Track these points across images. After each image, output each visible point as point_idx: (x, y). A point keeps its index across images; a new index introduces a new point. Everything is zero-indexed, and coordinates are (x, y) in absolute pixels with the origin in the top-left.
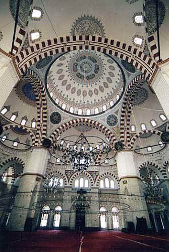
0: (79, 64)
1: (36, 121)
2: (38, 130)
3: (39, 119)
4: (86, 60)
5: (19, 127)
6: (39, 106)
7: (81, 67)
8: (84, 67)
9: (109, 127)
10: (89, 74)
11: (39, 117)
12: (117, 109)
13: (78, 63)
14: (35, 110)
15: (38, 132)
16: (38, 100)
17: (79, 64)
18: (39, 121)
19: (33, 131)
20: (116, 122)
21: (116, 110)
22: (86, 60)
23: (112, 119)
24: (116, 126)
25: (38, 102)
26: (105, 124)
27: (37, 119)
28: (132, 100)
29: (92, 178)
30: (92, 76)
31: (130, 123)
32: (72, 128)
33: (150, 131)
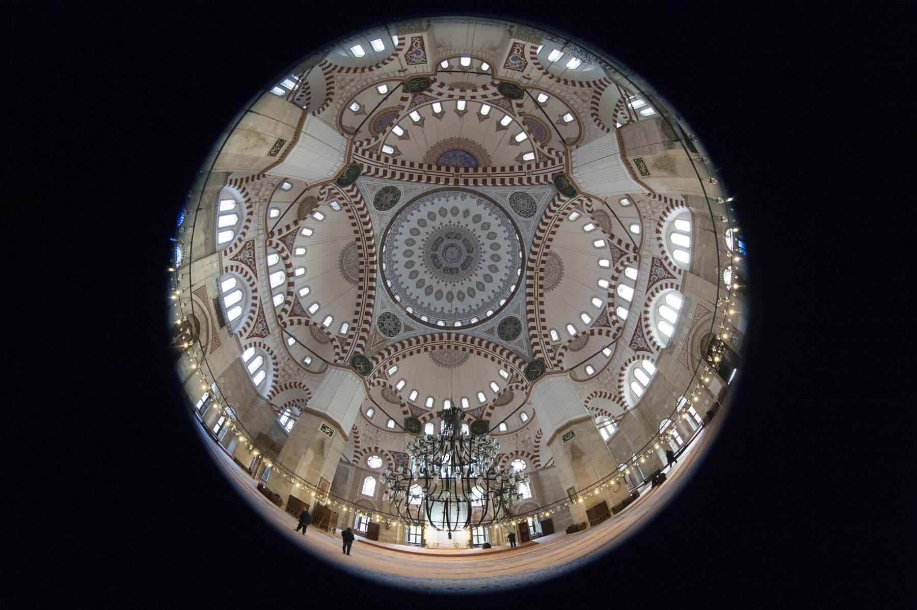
0: (459, 243)
1: (393, 155)
2: (378, 158)
3: (399, 163)
4: (465, 254)
5: (395, 121)
6: (425, 167)
7: (452, 245)
8: (452, 249)
9: (375, 322)
10: (440, 258)
11: (403, 163)
12: (414, 327)
14: (418, 159)
15: (375, 156)
16: (439, 168)
18: (395, 162)
19: (377, 145)
20: (390, 333)
21: (412, 326)
22: (465, 254)
25: (434, 168)
26: (378, 312)
28: (441, 347)
29: (252, 324)
31: (402, 361)
32: (352, 238)
33: (400, 398)
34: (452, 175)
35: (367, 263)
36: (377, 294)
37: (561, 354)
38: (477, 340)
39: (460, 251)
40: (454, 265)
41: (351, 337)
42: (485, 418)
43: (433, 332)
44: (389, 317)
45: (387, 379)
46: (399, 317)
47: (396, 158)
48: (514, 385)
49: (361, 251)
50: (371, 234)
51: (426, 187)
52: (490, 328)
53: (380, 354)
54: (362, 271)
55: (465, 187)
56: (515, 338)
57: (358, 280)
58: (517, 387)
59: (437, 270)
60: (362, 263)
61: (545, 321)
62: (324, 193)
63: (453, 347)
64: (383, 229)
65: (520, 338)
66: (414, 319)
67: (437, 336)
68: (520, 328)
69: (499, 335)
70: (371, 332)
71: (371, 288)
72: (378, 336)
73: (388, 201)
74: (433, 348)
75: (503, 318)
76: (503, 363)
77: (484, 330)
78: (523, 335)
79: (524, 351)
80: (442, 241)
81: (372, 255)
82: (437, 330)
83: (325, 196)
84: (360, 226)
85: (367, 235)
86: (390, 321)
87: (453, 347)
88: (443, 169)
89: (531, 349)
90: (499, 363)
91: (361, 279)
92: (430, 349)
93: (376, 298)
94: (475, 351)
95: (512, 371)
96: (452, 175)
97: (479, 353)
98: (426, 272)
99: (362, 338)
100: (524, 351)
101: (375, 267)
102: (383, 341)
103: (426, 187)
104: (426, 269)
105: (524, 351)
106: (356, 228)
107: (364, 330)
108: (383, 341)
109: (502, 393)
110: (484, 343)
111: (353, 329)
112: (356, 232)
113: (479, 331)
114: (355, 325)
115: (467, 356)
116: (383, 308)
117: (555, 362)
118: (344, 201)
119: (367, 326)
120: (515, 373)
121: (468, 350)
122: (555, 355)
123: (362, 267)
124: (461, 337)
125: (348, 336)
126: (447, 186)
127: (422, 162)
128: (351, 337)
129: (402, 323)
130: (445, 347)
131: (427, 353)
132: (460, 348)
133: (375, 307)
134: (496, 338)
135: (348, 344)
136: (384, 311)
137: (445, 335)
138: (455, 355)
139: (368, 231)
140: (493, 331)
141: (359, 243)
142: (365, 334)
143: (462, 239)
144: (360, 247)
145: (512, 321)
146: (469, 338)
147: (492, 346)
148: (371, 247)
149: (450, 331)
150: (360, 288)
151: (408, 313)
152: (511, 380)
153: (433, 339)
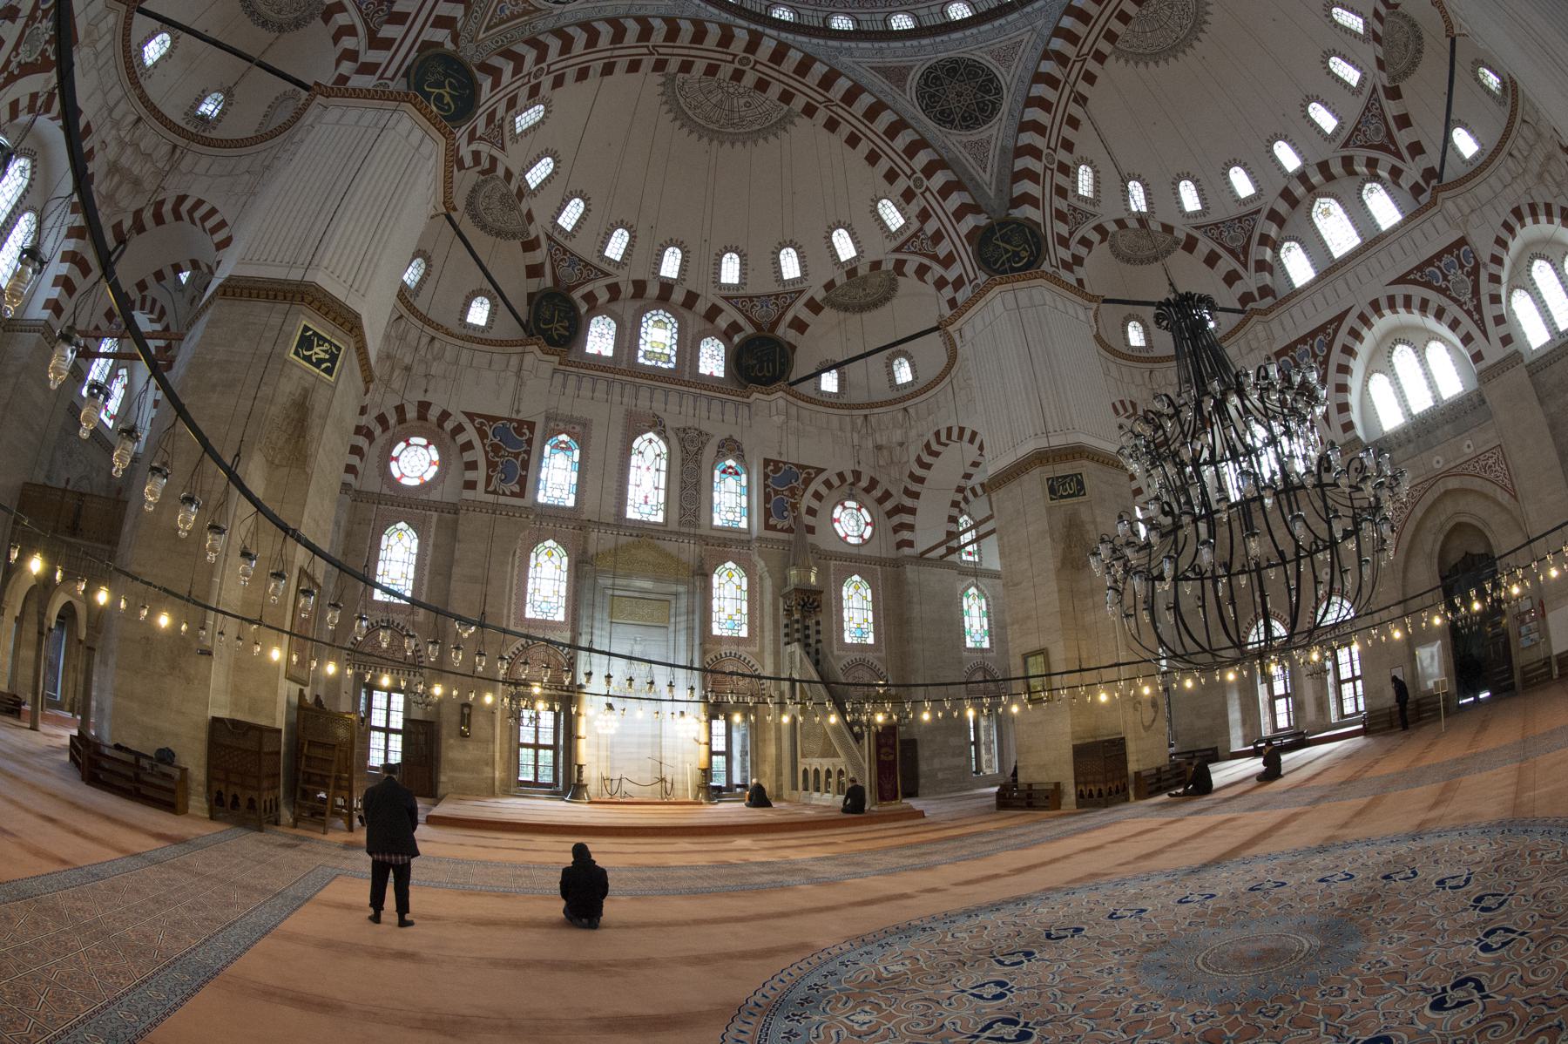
28: (712, 70)
37: (1085, 242)
38: (843, 85)
42: (784, 332)
45: (503, 148)
48: (913, 262)
52: (891, 61)
56: (968, 128)
58: (922, 271)
61: (1076, 129)
63: (750, 79)
65: (985, 136)
67: (714, 32)
68: (995, 109)
69: (920, 96)
74: (686, 67)
75: (952, 54)
76: (902, 183)
77: (877, 61)
78: (996, 132)
79: (987, 177)
87: (750, 79)
89: (1008, 181)
90: (891, 176)
92: (673, 65)
94: (822, 115)
95: (924, 216)
97: (832, 125)
100: (987, 177)
105: (987, 178)
109: (863, 270)
110: (865, 100)
113: (859, 61)
117: (1066, 255)
120: (931, 227)
121: (799, 102)
122: (1071, 234)
124: (794, 57)
130: (726, 71)
131: (657, 78)
132: (775, 90)
134: (907, 102)
137: (742, 37)
140: (905, 78)
145: (976, 75)
146: (819, 69)
147: (886, 118)
149: (760, 29)
152: (906, 242)
153: (699, 35)
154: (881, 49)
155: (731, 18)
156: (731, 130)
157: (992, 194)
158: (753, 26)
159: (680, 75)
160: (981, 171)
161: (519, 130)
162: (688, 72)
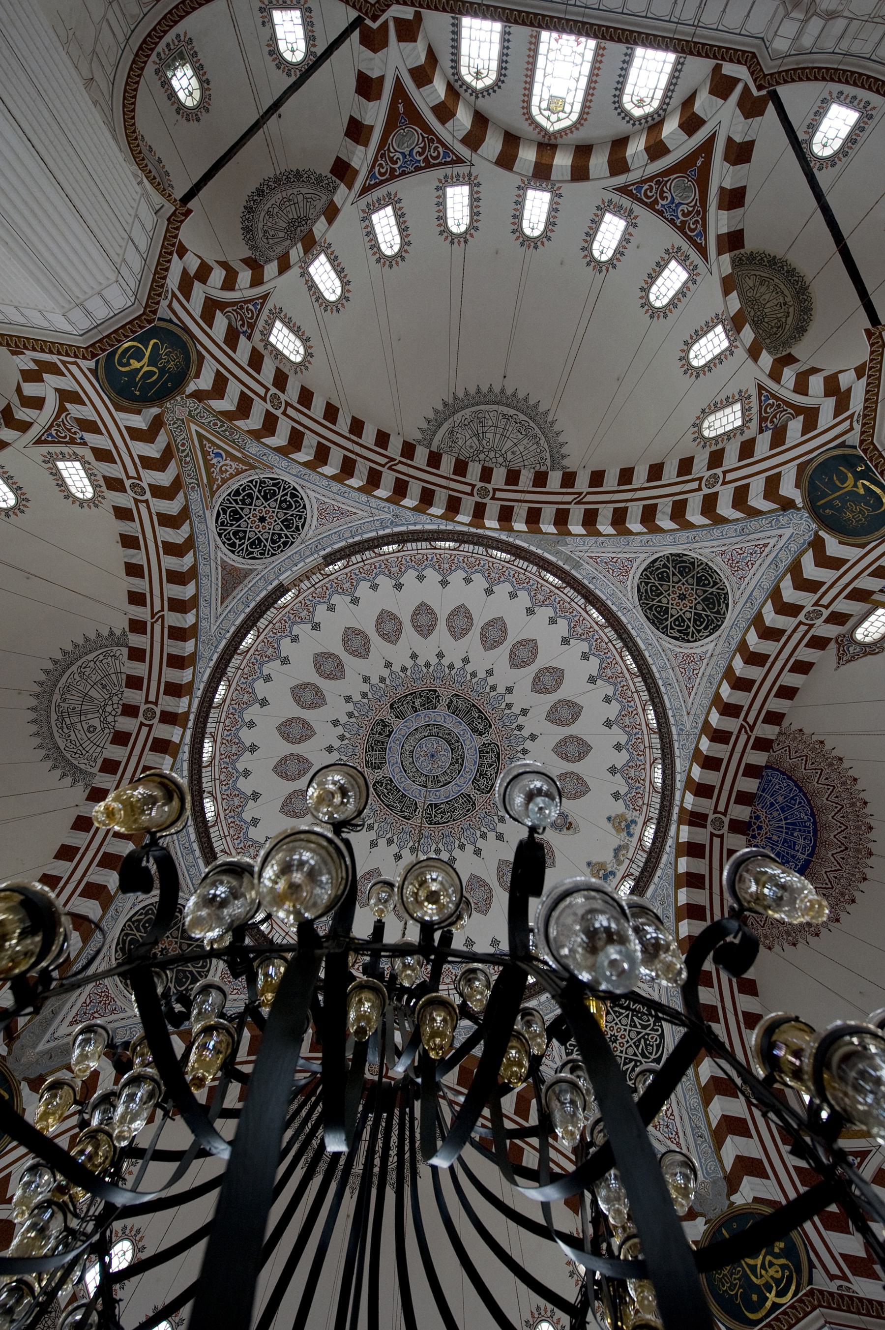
6: (769, 731)
8: (445, 757)
10: (424, 718)
11: (802, 668)
12: (231, 602)
13: (468, 788)
16: (752, 771)
17: (464, 784)
18: (819, 643)
21: (240, 593)
23: (264, 532)
24: (223, 494)
25: (759, 758)
27: (824, 658)
28: (134, 682)
30: (406, 708)
34: (721, 808)
35: (484, 492)
36: (374, 502)
39: (436, 780)
40: (394, 755)
41: (256, 361)
43: (200, 665)
44: (287, 524)
46: (282, 557)
47: (833, 645)
49: (526, 479)
50: (577, 529)
51: (688, 722)
53: (168, 454)
54: (461, 468)
55: (670, 842)
57: (434, 448)
59: (386, 701)
60: (486, 475)
62: (801, 387)
63: (127, 724)
64: (577, 565)
66: (259, 605)
70: (253, 448)
71: (401, 489)
72: (232, 466)
73: (670, 600)
74: (137, 654)
80: (475, 730)
81: (506, 515)
82: (205, 677)
83: (786, 387)
84: (628, 496)
85: (577, 513)
86: (274, 525)
87: (127, 724)
88: (750, 785)
91: (434, 460)
92: (137, 641)
93: (364, 498)
96: (721, 808)
98: (388, 665)
99: (244, 406)
101: (464, 518)
102: (211, 480)
103: (688, 722)
104: (396, 668)
106: (611, 481)
107: (270, 425)
108: (211, 480)
111: (280, 380)
112: (597, 478)
114: (292, 393)
115: (76, 773)
116: (323, 513)
118: (731, 458)
119: (280, 439)
123: (474, 471)
125: (260, 347)
126: (679, 785)
127: (785, 723)
128: (256, 361)
129: (257, 564)
130: (134, 697)
132: (117, 753)
133: (336, 486)
135: (232, 338)
136: (312, 514)
137: (181, 705)
138: (92, 729)
139: (590, 519)
141: (555, 480)
142: (255, 421)
143: (474, 794)
144: (540, 479)
148: (533, 517)
149: (190, 724)
150: (408, 450)
151: (281, 590)
153: (177, 662)
154: (193, 851)
155: (199, 693)
156: (54, 717)
157: (42, 1047)
158: (192, 717)
159: (125, 651)
160: (70, 1018)
161: (60, 465)
162: (130, 658)
